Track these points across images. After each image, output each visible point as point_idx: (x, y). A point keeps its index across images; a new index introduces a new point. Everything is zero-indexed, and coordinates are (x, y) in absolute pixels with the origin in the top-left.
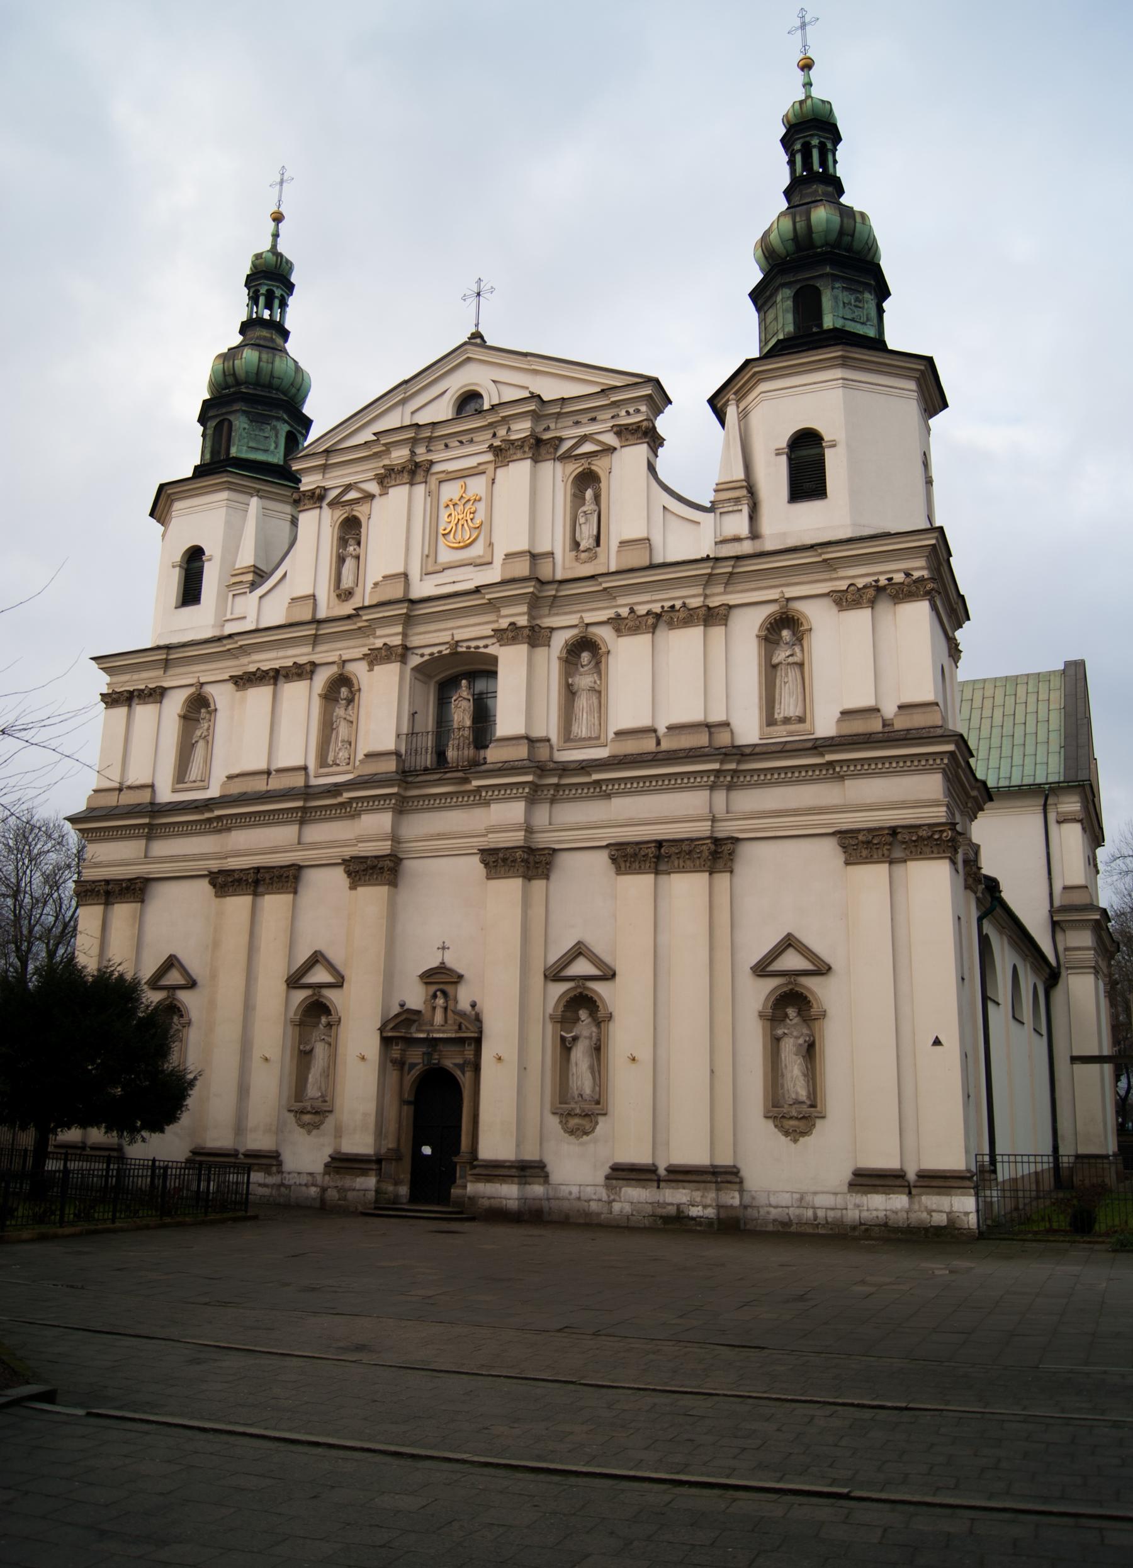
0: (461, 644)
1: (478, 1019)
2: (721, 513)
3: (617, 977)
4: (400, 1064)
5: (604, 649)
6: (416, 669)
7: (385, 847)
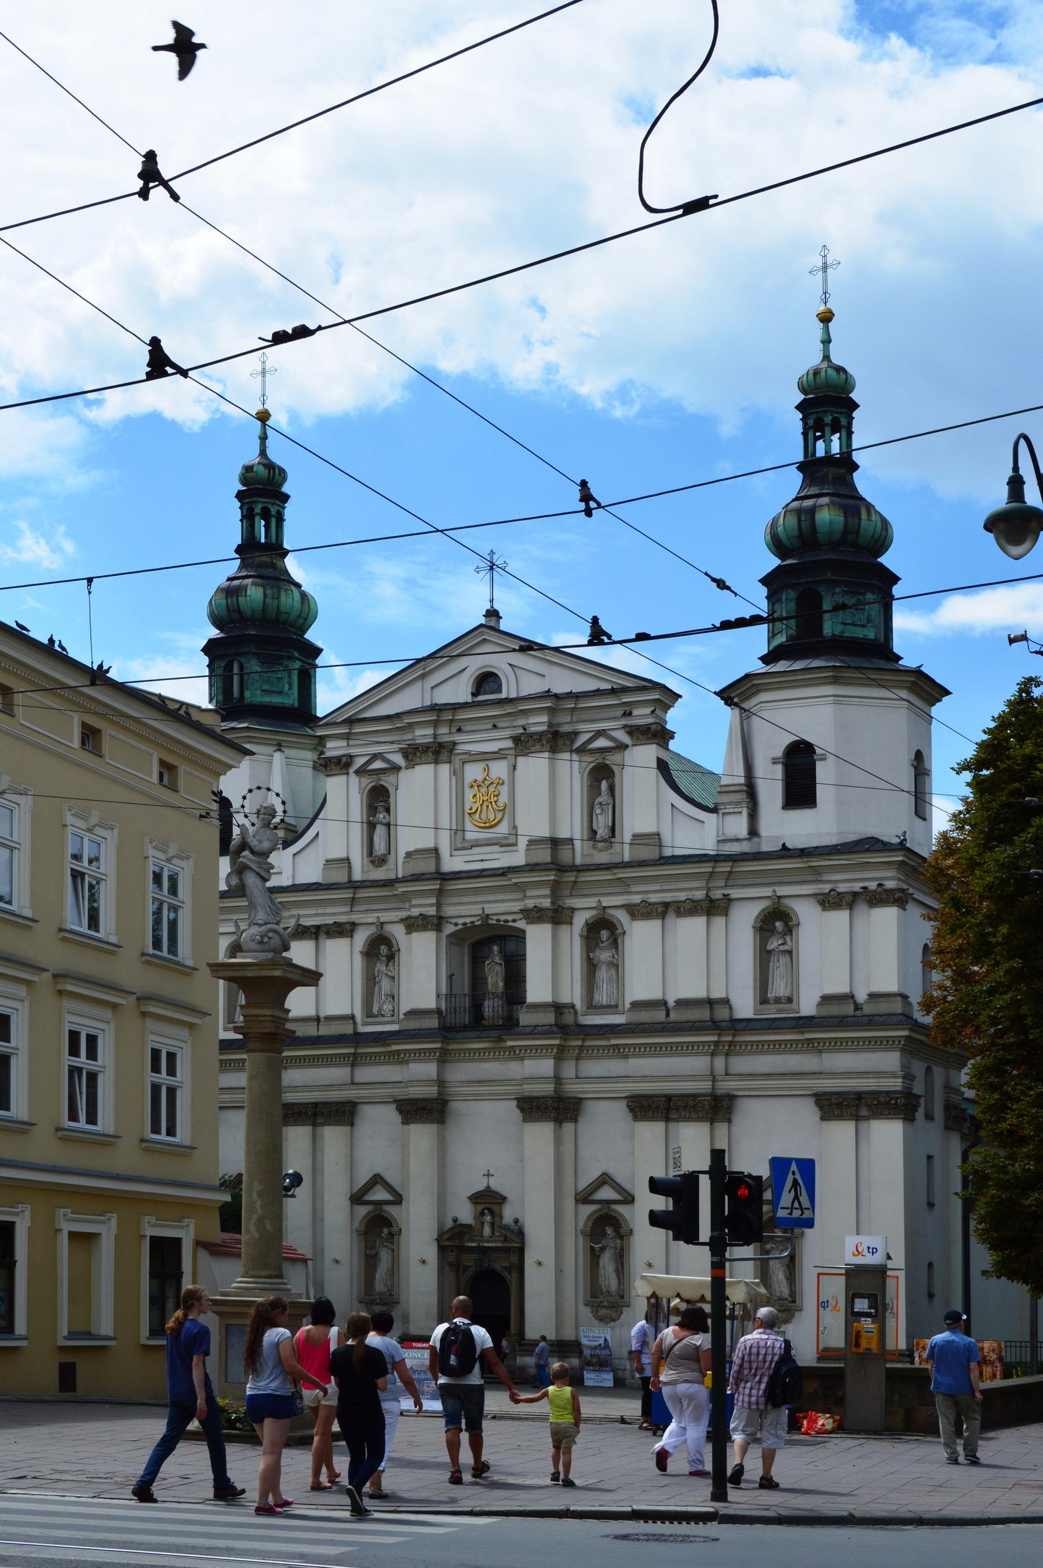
0: (491, 917)
1: (520, 1233)
2: (723, 814)
3: (636, 1202)
4: (457, 1267)
5: (620, 931)
7: (432, 1091)
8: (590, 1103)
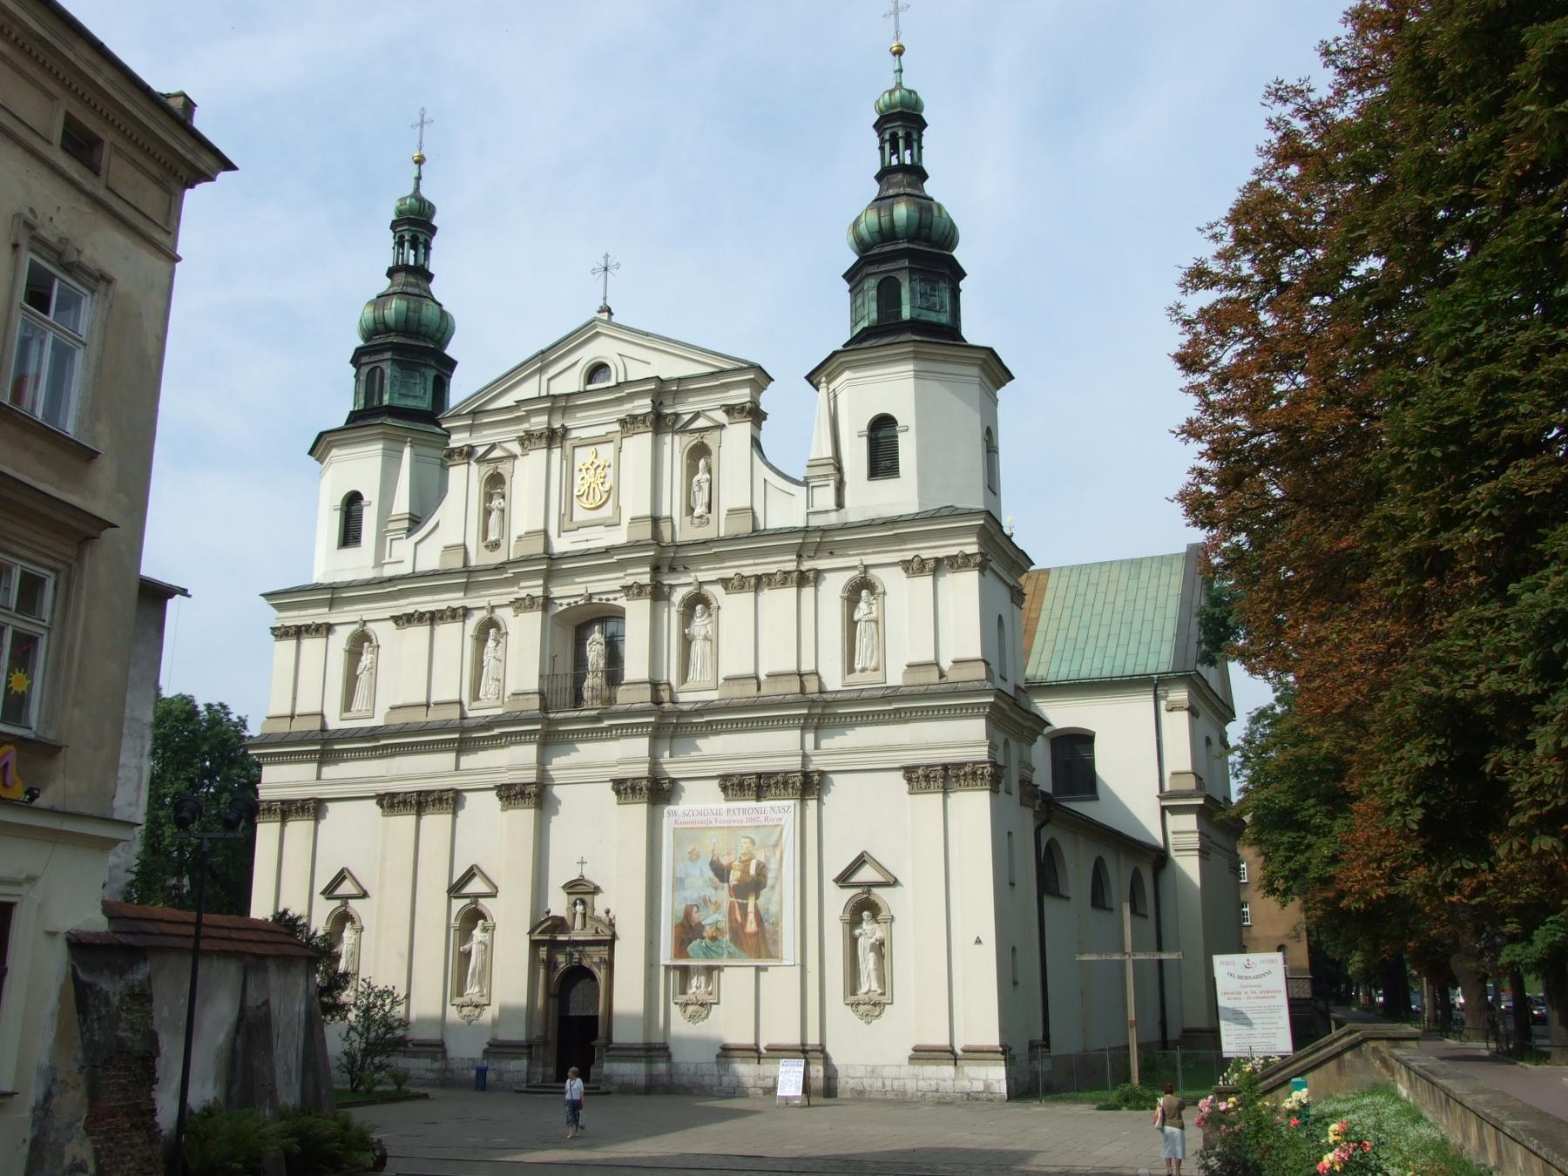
1: (611, 925)
7: (531, 776)
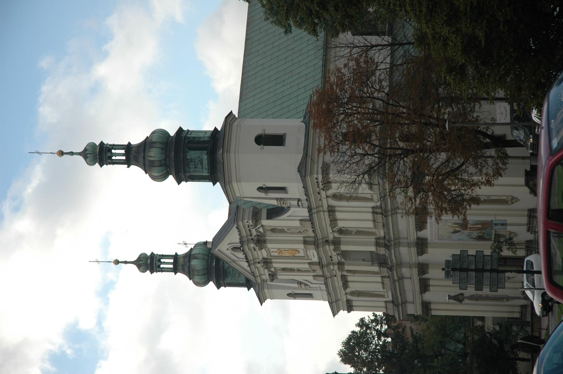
6: (345, 259)
8: (418, 236)
